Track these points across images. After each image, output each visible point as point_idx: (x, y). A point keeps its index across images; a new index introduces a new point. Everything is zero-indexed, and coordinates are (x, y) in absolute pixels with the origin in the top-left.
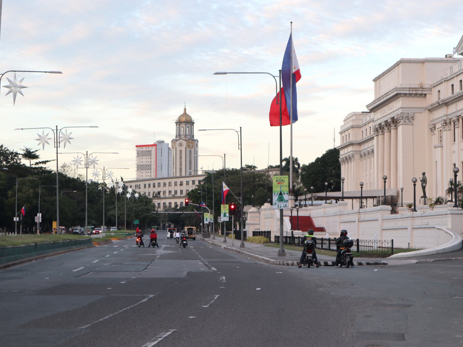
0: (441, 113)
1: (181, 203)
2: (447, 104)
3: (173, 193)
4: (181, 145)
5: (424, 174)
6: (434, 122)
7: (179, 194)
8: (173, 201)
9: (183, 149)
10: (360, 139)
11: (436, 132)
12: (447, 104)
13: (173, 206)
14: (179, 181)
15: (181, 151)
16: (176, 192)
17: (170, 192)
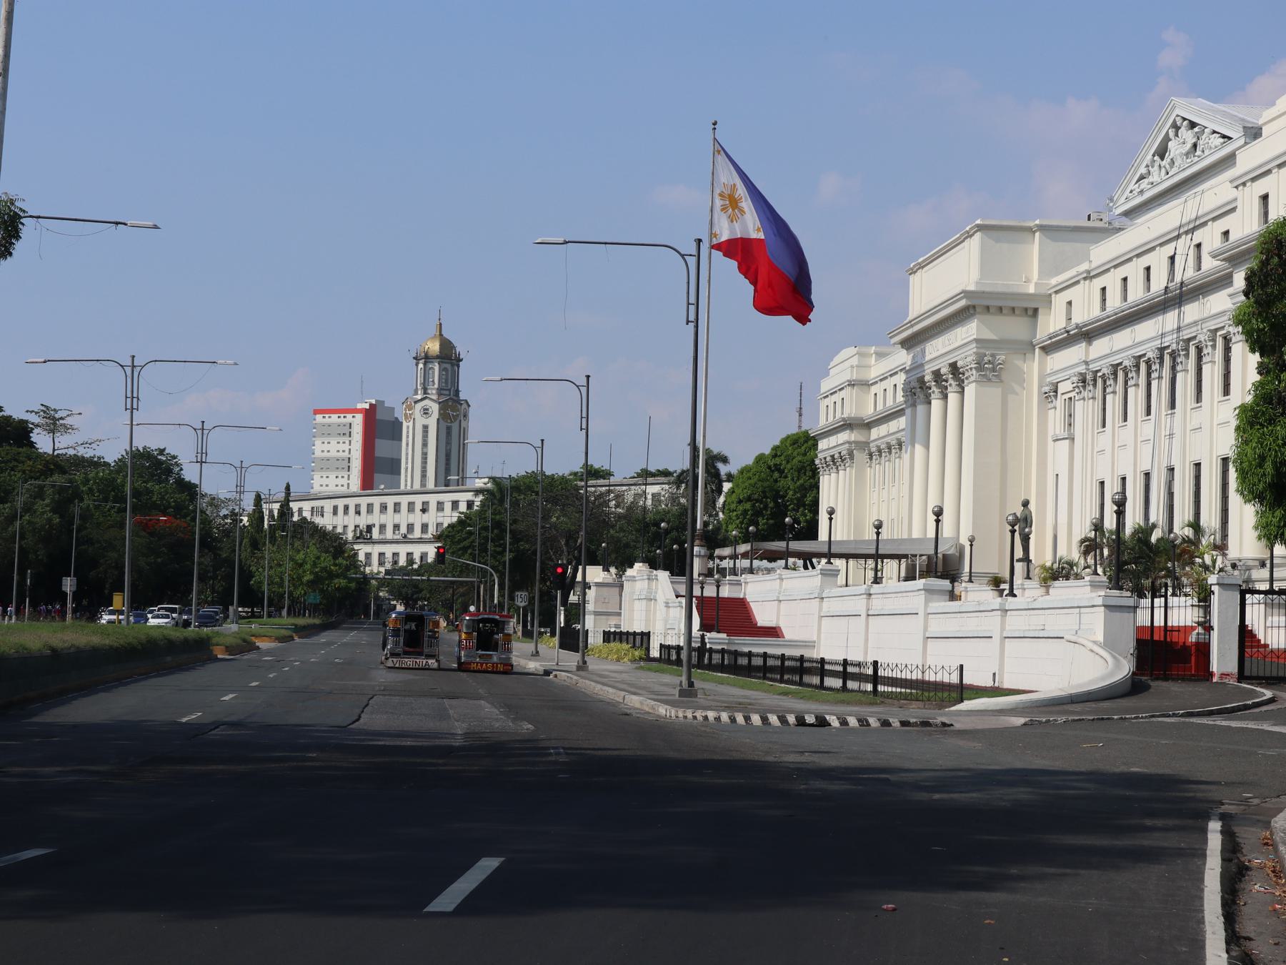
0: (1073, 356)
1: (423, 556)
2: (1087, 334)
3: (403, 530)
4: (426, 412)
5: (1026, 504)
6: (1054, 379)
7: (417, 533)
8: (403, 550)
9: (432, 422)
10: (868, 411)
11: (1059, 402)
12: (1087, 334)
13: (402, 561)
14: (418, 500)
15: (425, 428)
16: (410, 527)
17: (396, 527)
